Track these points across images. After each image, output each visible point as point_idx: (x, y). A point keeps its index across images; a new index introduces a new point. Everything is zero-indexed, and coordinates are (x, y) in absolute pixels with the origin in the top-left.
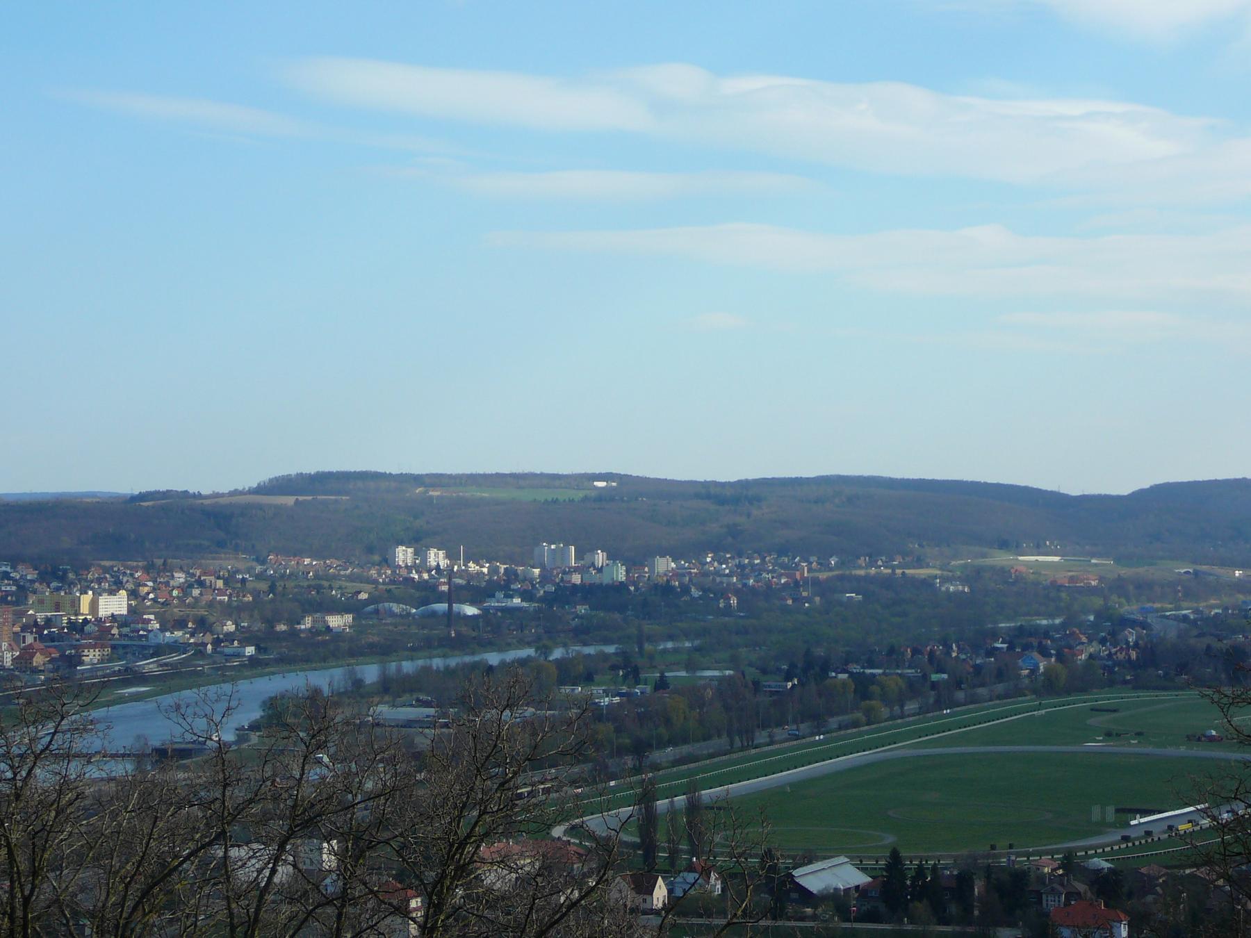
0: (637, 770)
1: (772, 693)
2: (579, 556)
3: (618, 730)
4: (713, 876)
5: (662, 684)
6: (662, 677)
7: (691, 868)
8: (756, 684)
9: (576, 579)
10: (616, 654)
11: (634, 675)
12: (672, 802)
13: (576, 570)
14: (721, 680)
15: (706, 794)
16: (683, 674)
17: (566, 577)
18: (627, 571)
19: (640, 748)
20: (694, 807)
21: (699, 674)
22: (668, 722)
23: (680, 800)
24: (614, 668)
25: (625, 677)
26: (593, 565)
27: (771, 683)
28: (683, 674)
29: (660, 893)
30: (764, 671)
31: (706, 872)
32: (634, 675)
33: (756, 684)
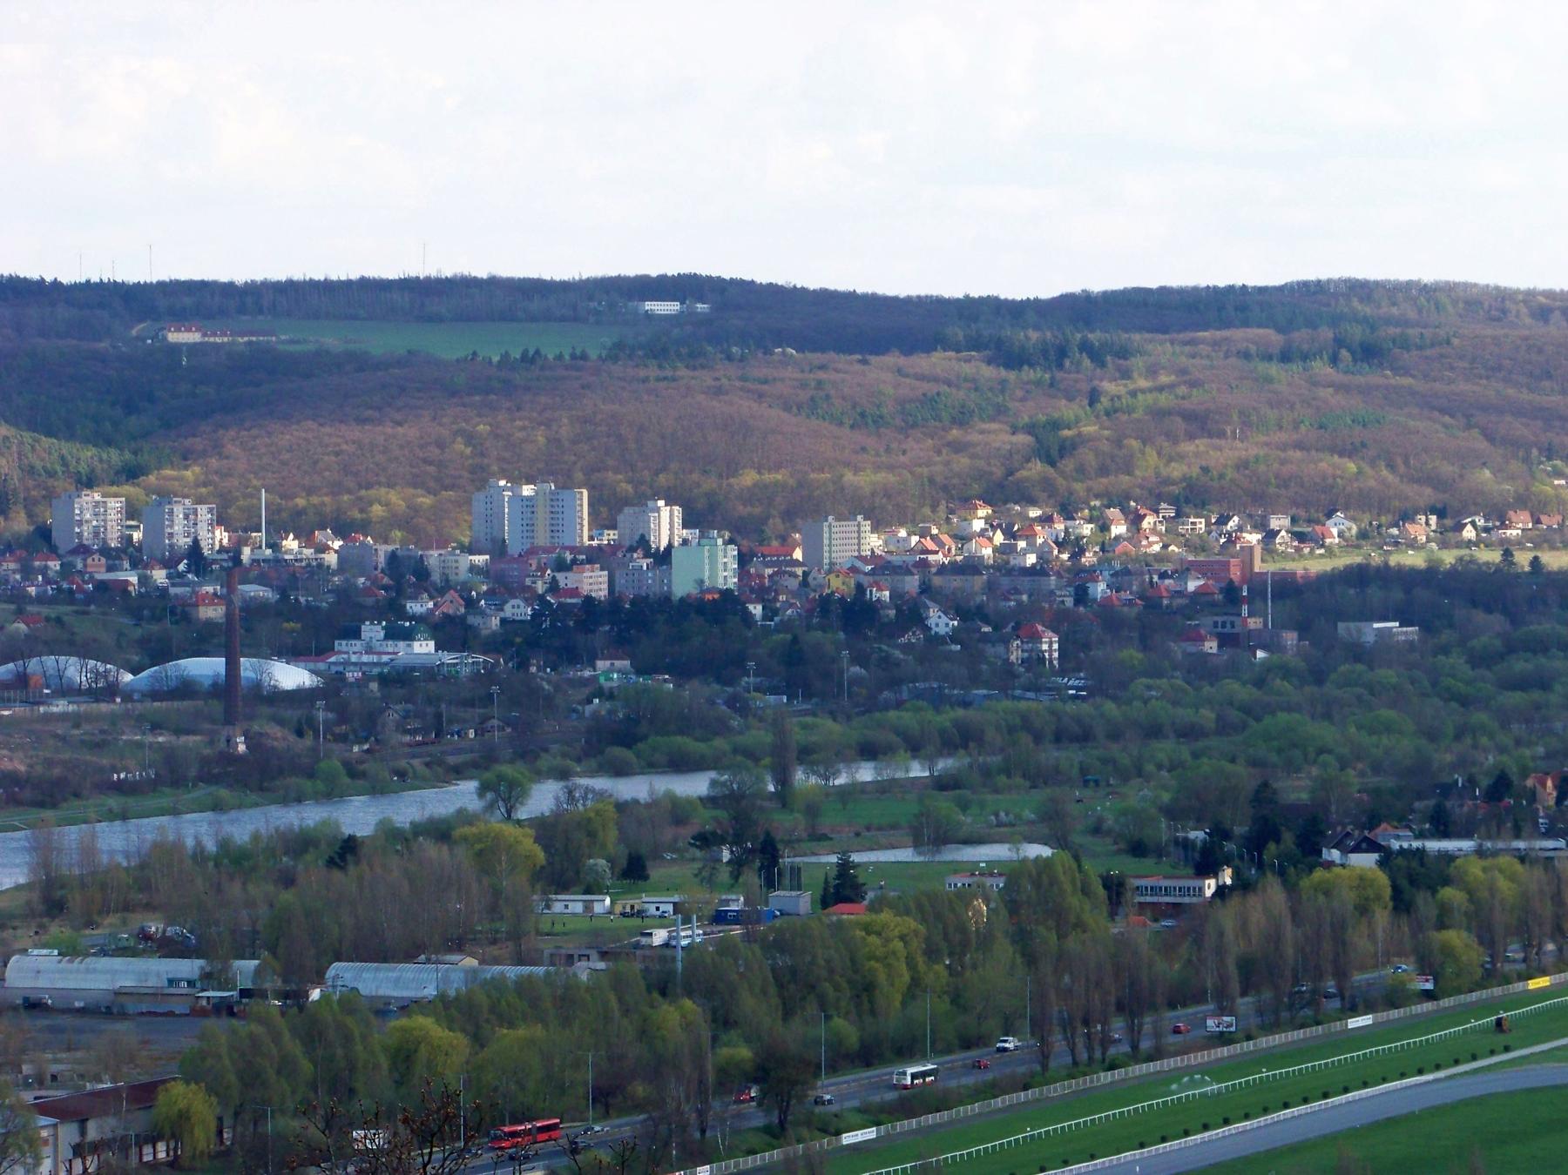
0: (776, 1134)
1: (1158, 912)
3: (723, 1020)
5: (843, 888)
6: (844, 867)
9: (594, 582)
10: (710, 801)
11: (766, 859)
14: (1015, 874)
16: (905, 855)
17: (566, 580)
18: (743, 559)
22: (865, 990)
24: (705, 840)
25: (737, 864)
26: (643, 543)
28: (905, 855)
30: (1138, 849)
32: (766, 859)
33: (1115, 889)
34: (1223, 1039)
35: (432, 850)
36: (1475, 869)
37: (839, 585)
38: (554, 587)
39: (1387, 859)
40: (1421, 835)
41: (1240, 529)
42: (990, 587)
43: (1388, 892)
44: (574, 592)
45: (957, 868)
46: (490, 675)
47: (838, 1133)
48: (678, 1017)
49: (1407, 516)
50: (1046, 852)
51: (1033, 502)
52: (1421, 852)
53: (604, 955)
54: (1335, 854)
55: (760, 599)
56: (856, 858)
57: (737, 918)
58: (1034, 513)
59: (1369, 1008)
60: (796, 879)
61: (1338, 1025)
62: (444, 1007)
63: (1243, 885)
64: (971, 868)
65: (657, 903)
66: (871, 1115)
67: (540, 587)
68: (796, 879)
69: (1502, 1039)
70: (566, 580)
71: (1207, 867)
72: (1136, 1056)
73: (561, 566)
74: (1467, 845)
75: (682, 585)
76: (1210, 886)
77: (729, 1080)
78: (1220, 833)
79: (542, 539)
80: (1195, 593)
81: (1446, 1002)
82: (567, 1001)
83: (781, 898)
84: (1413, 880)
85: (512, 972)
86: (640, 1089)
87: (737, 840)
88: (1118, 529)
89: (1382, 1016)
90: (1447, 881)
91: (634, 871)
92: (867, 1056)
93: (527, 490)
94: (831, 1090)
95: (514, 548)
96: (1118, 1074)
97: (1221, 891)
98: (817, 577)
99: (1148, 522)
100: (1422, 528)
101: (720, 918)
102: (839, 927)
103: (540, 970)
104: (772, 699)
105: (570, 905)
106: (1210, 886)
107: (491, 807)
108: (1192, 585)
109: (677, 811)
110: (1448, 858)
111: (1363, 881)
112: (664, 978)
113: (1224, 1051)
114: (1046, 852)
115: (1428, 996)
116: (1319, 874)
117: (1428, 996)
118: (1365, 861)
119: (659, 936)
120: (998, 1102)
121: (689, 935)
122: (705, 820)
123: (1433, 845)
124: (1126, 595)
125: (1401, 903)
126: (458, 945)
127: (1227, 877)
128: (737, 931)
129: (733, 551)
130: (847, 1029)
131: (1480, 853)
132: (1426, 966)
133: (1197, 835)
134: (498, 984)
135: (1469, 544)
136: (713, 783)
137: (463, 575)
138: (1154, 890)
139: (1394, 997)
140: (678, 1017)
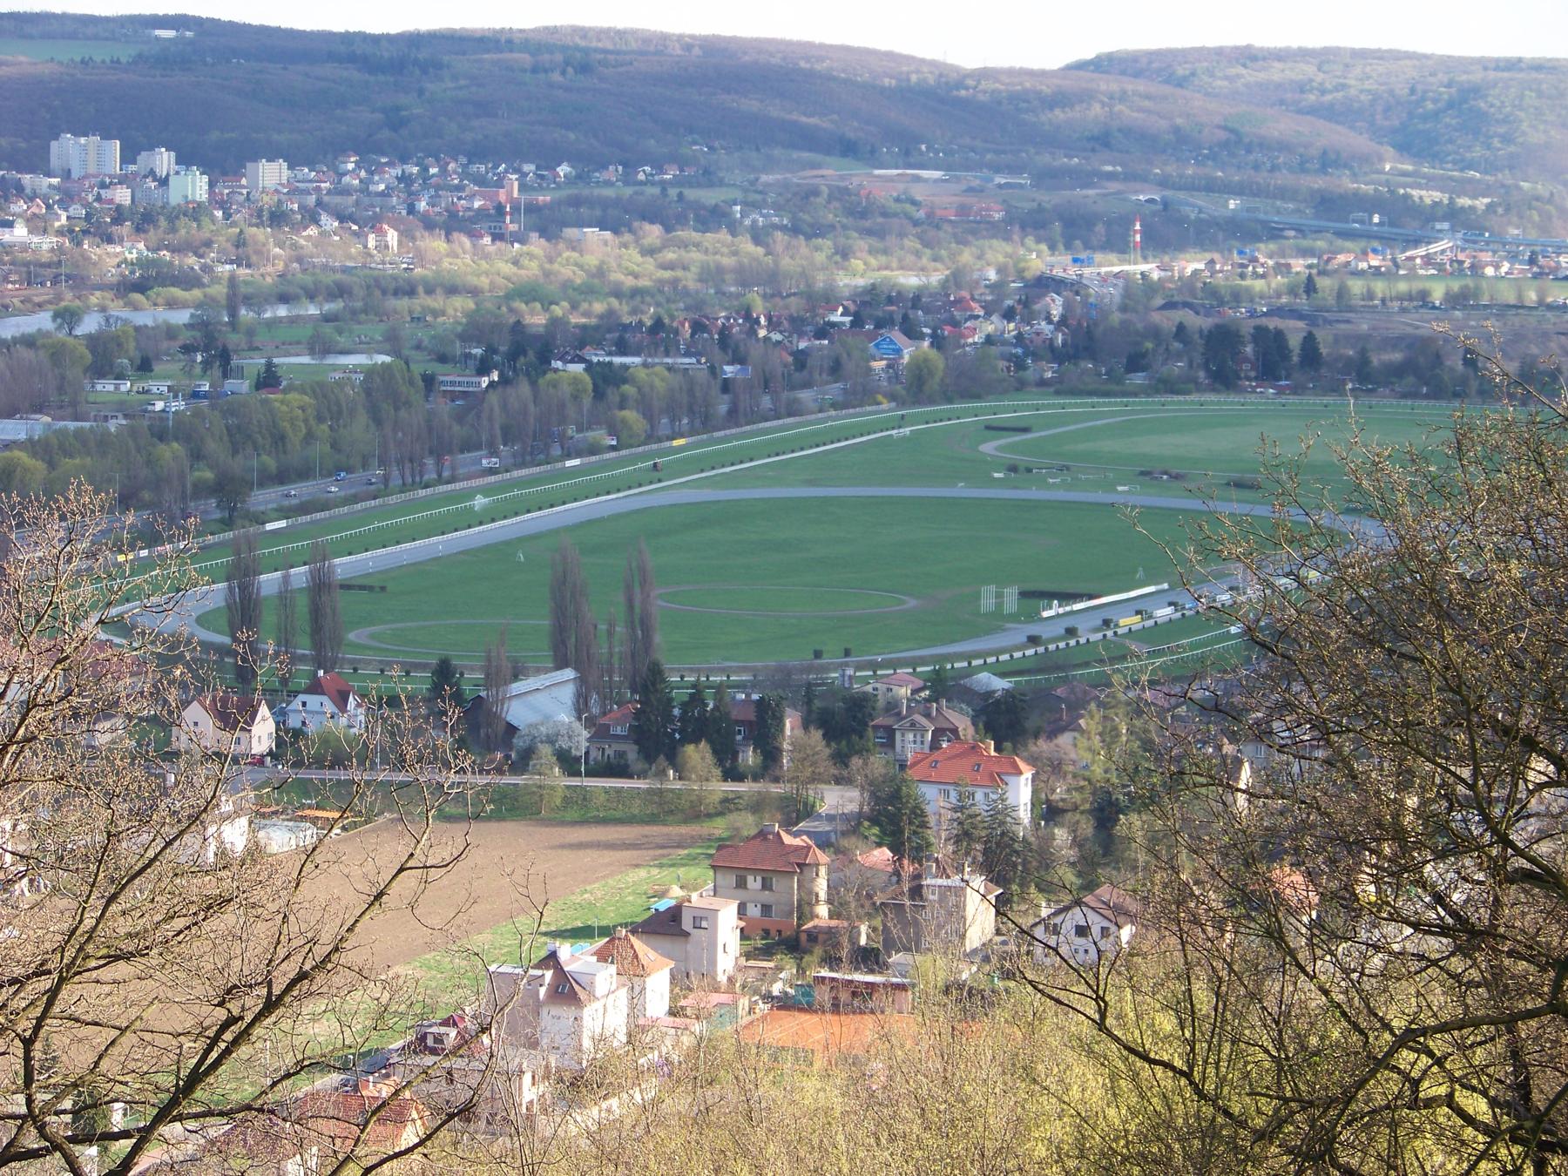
0: (228, 524)
1: (453, 396)
2: (128, 157)
3: (197, 456)
4: (351, 702)
5: (268, 380)
6: (269, 365)
7: (315, 688)
8: (429, 381)
9: (123, 195)
10: (189, 326)
11: (222, 360)
12: (286, 579)
13: (123, 180)
14: (370, 372)
15: (343, 566)
16: (306, 360)
17: (105, 193)
18: (211, 184)
19: (228, 494)
20: (321, 585)
21: (332, 360)
22: (280, 439)
23: (300, 573)
24: (188, 349)
25: (207, 364)
26: (152, 173)
27: (450, 377)
28: (306, 360)
29: (262, 733)
30: (443, 359)
31: (341, 700)
32: (222, 360)
33: (429, 381)
34: (492, 471)
35: (25, 354)
36: (642, 374)
37: (267, 201)
38: (99, 198)
39: (590, 367)
40: (610, 354)
41: (506, 171)
42: (357, 203)
43: (590, 387)
44: (111, 201)
45: (335, 368)
46: (60, 249)
47: (264, 523)
48: (171, 453)
49: (603, 166)
50: (388, 359)
51: (384, 154)
52: (610, 363)
53: (126, 416)
54: (558, 364)
55: (221, 207)
56: (275, 360)
57: (206, 395)
58: (384, 160)
59: (578, 455)
60: (240, 373)
61: (559, 465)
62: (30, 445)
63: (504, 381)
64: (344, 369)
65: (158, 386)
66: (284, 513)
67: (90, 198)
68: (240, 373)
69: (657, 475)
70: (105, 193)
71: (483, 370)
72: (441, 481)
73: (103, 186)
74: (637, 360)
75: (175, 197)
76: (485, 382)
77: (201, 490)
78: (491, 350)
79: (92, 169)
80: (479, 209)
81: (623, 452)
82: (103, 443)
83: (231, 384)
84: (605, 378)
85: (72, 425)
86: (146, 495)
87: (206, 349)
88: (433, 171)
89: (586, 460)
90: (625, 381)
91: (144, 367)
92: (281, 478)
93: (83, 140)
94: (263, 498)
95: (75, 175)
96: (429, 491)
97: (491, 384)
98: (255, 195)
99: (452, 166)
100: (613, 172)
101: (196, 395)
102: (265, 402)
103: (87, 425)
104: (228, 267)
105: (106, 386)
106: (485, 382)
107: (59, 328)
108: (477, 204)
109: (171, 332)
110: (625, 367)
111: (575, 380)
112: (161, 430)
113: (492, 479)
114: (388, 359)
115: (613, 448)
116: (550, 376)
117: (613, 448)
118: (578, 368)
119: (159, 406)
120: (358, 506)
121: (178, 405)
122: (186, 337)
123: (617, 360)
124: (437, 209)
125: (599, 394)
126: (39, 409)
127: (495, 376)
128: (206, 402)
129: (205, 178)
130: (270, 462)
131: (645, 365)
132: (612, 432)
133: (478, 351)
134: (63, 433)
135: (641, 183)
136: (192, 316)
137: (45, 190)
138: (453, 383)
139: (594, 450)
140: (171, 453)
